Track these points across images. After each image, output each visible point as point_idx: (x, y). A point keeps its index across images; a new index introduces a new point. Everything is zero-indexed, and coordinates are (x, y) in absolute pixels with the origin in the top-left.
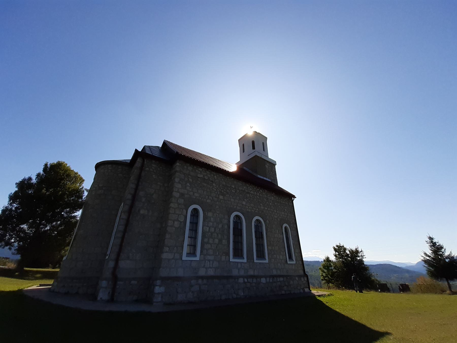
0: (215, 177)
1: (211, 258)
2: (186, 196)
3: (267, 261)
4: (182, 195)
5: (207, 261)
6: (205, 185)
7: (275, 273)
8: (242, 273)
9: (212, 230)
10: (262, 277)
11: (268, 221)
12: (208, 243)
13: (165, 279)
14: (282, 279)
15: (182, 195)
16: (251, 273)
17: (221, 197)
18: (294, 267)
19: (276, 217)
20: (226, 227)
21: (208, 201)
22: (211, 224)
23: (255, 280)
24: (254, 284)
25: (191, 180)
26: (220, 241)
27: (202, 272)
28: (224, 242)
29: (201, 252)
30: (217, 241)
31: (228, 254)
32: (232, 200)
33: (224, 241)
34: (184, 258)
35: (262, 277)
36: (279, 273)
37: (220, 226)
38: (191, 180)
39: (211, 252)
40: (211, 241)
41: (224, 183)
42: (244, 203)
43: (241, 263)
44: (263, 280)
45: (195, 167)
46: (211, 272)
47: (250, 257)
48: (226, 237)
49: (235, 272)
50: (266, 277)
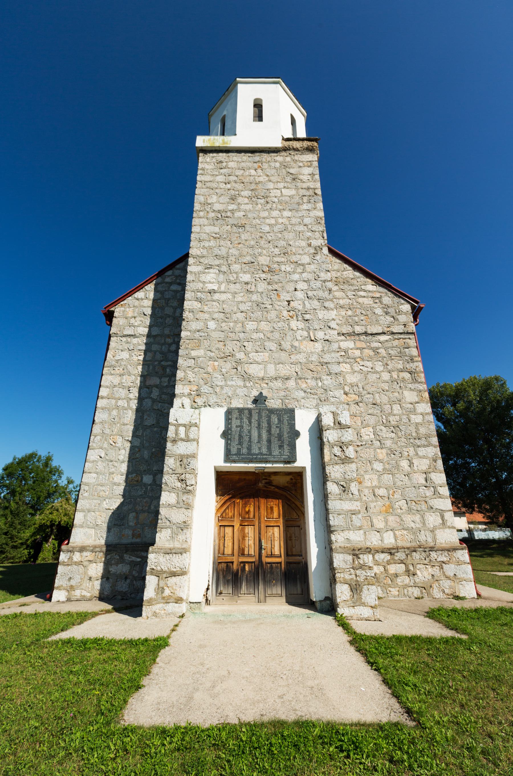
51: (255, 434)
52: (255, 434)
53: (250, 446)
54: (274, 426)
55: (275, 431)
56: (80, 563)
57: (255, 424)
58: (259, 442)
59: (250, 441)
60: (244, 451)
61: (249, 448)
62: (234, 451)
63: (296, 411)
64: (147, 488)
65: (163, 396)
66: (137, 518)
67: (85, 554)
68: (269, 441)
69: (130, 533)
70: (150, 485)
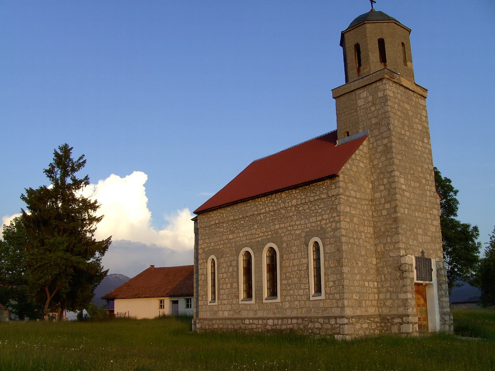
1: (226, 302)
5: (223, 305)
6: (217, 230)
7: (289, 313)
8: (251, 315)
10: (269, 319)
11: (284, 245)
12: (222, 289)
14: (294, 321)
16: (260, 314)
17: (231, 237)
18: (321, 304)
19: (298, 232)
20: (235, 268)
21: (221, 246)
23: (260, 322)
24: (260, 326)
26: (232, 284)
27: (220, 315)
28: (235, 285)
30: (229, 285)
31: (238, 297)
33: (234, 284)
35: (269, 319)
36: (294, 314)
37: (231, 270)
41: (232, 218)
43: (250, 304)
44: (270, 322)
46: (226, 314)
49: (244, 314)
50: (273, 319)
51: (423, 269)
52: (423, 269)
53: (422, 274)
54: (427, 266)
55: (427, 268)
56: (352, 324)
57: (423, 265)
58: (424, 273)
59: (422, 272)
60: (421, 276)
61: (422, 275)
62: (418, 276)
63: (432, 260)
64: (367, 288)
65: (367, 238)
66: (365, 303)
67: (353, 320)
68: (426, 273)
69: (364, 310)
70: (368, 287)
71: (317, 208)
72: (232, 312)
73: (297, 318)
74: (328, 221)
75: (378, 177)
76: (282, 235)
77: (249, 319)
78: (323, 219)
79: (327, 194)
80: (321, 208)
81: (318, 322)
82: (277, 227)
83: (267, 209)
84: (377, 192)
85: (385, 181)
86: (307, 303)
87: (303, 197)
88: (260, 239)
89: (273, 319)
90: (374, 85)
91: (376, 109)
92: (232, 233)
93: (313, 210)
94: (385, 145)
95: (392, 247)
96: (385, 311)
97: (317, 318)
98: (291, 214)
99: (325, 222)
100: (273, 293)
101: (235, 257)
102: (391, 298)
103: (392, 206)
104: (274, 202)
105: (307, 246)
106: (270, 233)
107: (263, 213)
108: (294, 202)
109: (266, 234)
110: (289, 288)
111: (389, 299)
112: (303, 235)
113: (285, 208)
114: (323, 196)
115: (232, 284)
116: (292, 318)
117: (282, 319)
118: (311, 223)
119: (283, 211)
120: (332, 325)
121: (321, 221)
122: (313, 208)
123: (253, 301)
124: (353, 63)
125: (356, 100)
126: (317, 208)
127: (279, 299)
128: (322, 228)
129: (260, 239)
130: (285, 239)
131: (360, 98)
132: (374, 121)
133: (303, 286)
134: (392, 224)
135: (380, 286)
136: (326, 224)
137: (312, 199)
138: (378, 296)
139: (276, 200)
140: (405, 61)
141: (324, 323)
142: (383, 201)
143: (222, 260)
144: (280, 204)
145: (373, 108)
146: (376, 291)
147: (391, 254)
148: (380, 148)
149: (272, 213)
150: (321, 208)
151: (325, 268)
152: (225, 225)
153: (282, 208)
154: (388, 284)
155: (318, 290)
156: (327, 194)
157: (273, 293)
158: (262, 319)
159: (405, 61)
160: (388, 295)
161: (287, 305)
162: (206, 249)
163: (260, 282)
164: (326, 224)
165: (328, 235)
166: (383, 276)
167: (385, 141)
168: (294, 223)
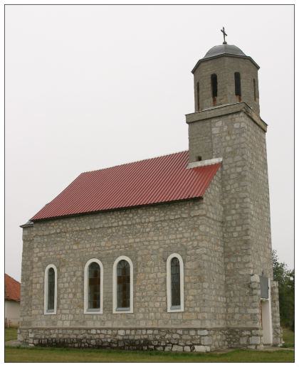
0: (68, 225)
1: (68, 312)
2: (43, 258)
3: (132, 311)
4: (40, 258)
7: (143, 324)
8: (98, 325)
9: (67, 285)
10: (120, 329)
11: (139, 259)
13: (33, 329)
15: (40, 258)
16: (109, 325)
17: (75, 247)
18: (180, 316)
19: (155, 247)
20: (80, 279)
22: (65, 280)
23: (110, 332)
25: (46, 240)
26: (75, 294)
27: (59, 324)
29: (58, 308)
30: (71, 296)
32: (88, 246)
34: (45, 313)
35: (120, 329)
36: (150, 325)
37: (74, 279)
38: (46, 240)
39: (66, 306)
40: (66, 296)
41: (78, 229)
42: (103, 244)
45: (48, 224)
46: (67, 324)
47: (108, 308)
48: (79, 290)
49: (90, 324)
71: (178, 226)
72: (74, 322)
73: (153, 329)
74: (189, 239)
75: (230, 201)
76: (137, 249)
77: (96, 329)
78: (184, 237)
79: (189, 214)
80: (182, 227)
81: (176, 333)
82: (132, 241)
83: (120, 223)
84: (229, 216)
85: (237, 206)
86: (164, 315)
87: (163, 214)
88: (111, 251)
89: (125, 329)
90: (230, 117)
91: (231, 139)
92: (77, 243)
93: (173, 229)
94: (240, 173)
95: (242, 266)
96: (234, 324)
97: (176, 329)
98: (148, 230)
99: (185, 240)
100: (124, 302)
101: (80, 268)
102: (239, 313)
103: (244, 229)
104: (128, 217)
105: (166, 261)
106: (123, 246)
107: (115, 227)
108: (152, 219)
109: (118, 247)
110: (143, 300)
111: (237, 313)
112: (161, 250)
113: (140, 223)
114: (184, 216)
115: (75, 294)
116: (147, 329)
117: (136, 329)
118: (170, 240)
119: (139, 227)
120: (192, 336)
121: (181, 238)
122: (173, 226)
123: (101, 311)
124: (207, 90)
125: (211, 128)
126: (178, 226)
127: (131, 310)
128: (182, 245)
129: (111, 251)
130: (140, 253)
131: (215, 127)
132: (229, 149)
133: (159, 299)
134: (243, 245)
135: (228, 301)
136: (187, 242)
137: (172, 218)
138: (227, 311)
139: (131, 215)
140: (198, 83)
141: (184, 334)
142: (234, 224)
143: (63, 270)
144: (135, 220)
145: (228, 138)
146: (225, 305)
147: (241, 273)
148: (234, 175)
149: (126, 227)
150: (182, 227)
151: (185, 283)
152: (68, 235)
153: (139, 224)
154: (237, 300)
155: (176, 301)
156: (189, 214)
157: (124, 302)
158: (112, 329)
159: (198, 83)
160: (237, 310)
161: (141, 316)
162: (43, 258)
163: (109, 293)
164: (187, 242)
165: (189, 252)
166: (232, 292)
167: (239, 170)
168: (150, 239)
